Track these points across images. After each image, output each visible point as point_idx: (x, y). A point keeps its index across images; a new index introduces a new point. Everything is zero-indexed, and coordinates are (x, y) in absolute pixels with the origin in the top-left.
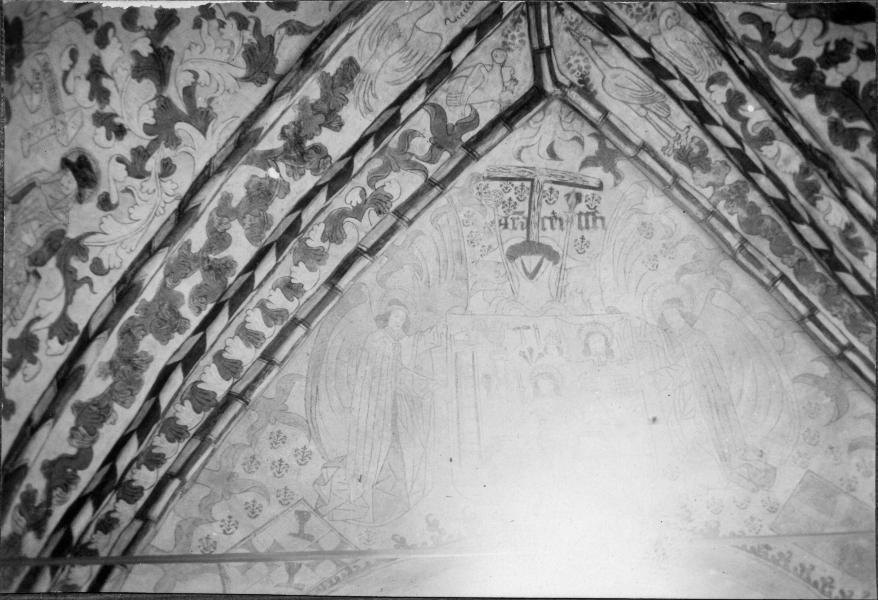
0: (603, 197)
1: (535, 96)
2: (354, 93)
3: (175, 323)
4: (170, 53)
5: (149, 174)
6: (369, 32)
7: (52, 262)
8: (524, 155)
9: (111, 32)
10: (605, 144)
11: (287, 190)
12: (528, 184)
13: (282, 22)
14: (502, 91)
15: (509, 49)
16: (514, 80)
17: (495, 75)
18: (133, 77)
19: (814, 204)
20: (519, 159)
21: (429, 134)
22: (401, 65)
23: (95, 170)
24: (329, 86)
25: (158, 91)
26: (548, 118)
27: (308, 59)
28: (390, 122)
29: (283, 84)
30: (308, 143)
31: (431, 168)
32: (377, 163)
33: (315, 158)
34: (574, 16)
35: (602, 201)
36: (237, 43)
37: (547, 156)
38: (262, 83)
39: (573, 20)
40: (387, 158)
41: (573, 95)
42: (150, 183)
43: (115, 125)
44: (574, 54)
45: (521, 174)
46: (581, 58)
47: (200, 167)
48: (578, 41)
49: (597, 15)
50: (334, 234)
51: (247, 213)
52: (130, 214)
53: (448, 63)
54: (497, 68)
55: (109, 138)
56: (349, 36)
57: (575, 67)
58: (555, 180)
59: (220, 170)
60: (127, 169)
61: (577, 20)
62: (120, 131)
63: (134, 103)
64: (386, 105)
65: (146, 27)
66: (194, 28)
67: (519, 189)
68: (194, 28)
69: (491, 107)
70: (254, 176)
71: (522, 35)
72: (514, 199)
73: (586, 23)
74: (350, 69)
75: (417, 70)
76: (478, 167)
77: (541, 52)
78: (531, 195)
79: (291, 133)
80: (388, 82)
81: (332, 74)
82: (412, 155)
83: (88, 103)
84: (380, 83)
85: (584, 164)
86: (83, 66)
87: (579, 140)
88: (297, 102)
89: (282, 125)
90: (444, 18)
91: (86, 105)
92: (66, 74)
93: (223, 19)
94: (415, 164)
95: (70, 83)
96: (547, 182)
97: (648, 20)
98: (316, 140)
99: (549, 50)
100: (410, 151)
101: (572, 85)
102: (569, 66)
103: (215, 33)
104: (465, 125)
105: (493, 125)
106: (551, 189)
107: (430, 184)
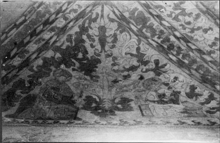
19: (48, 31)
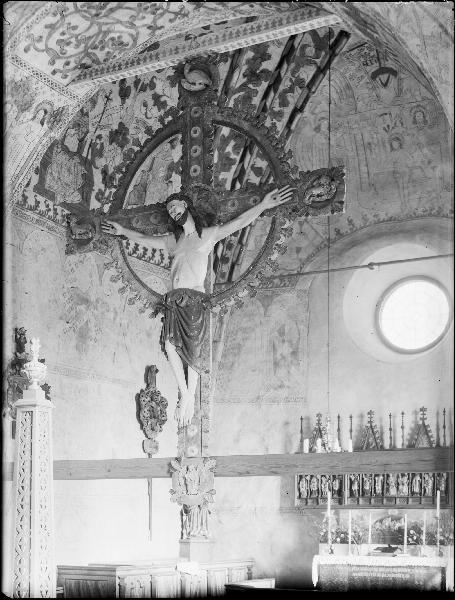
3: (232, 162)
7: (174, 174)
21: (312, 44)
50: (284, 103)
86: (151, 102)
92: (146, 113)
95: (149, 115)
98: (261, 68)
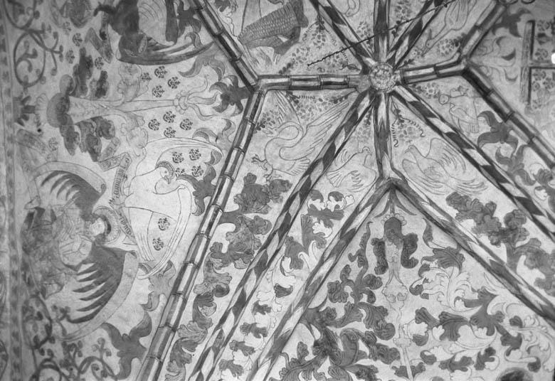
0: (538, 20)
1: (466, 74)
2: (471, 195)
4: (443, 315)
5: (519, 334)
6: (430, 189)
8: (512, 76)
9: (426, 353)
10: (499, 24)
11: (535, 240)
12: (534, 71)
13: (423, 242)
14: (467, 96)
15: (439, 93)
16: (459, 89)
17: (457, 101)
18: (457, 340)
20: (514, 80)
21: (498, 144)
22: (452, 165)
23: (513, 371)
24: (465, 213)
25: (466, 324)
26: (484, 62)
27: (447, 229)
28: (490, 171)
29: (463, 245)
30: (504, 226)
31: (521, 143)
32: (519, 179)
33: (514, 221)
34: (412, 55)
35: (542, 19)
36: (438, 271)
37: (513, 60)
38: (463, 257)
39: (416, 53)
40: (514, 173)
41: (466, 51)
42: (526, 334)
43: (486, 355)
44: (439, 51)
45: (526, 77)
46: (441, 46)
47: (516, 300)
48: (430, 49)
49: (409, 40)
51: (550, 267)
52: (544, 350)
53: (449, 134)
54: (453, 100)
55: (493, 360)
56: (432, 203)
57: (447, 49)
58: (529, 52)
59: (518, 289)
60: (515, 349)
61: (416, 51)
62: (490, 351)
63: (472, 341)
64: (479, 174)
65: (426, 330)
66: (428, 299)
67: (537, 77)
68: (428, 299)
69: (478, 103)
70: (525, 264)
71: (429, 86)
72: (544, 80)
73: (417, 44)
74: (455, 200)
75: (453, 153)
76: (520, 107)
77: (439, 72)
78: (541, 68)
79: (496, 238)
80: (464, 172)
81: (457, 212)
82: (512, 155)
83: (469, 372)
84: (466, 178)
85: (516, 34)
87: (498, 41)
88: (475, 235)
89: (490, 245)
90: (420, 138)
91: (470, 373)
93: (423, 280)
94: (518, 153)
96: (531, 58)
97: (410, 5)
98: (502, 220)
99: (437, 68)
100: (509, 157)
101: (459, 51)
102: (447, 53)
103: (431, 285)
104: (491, 120)
105: (490, 102)
106: (537, 54)
107: (531, 144)
